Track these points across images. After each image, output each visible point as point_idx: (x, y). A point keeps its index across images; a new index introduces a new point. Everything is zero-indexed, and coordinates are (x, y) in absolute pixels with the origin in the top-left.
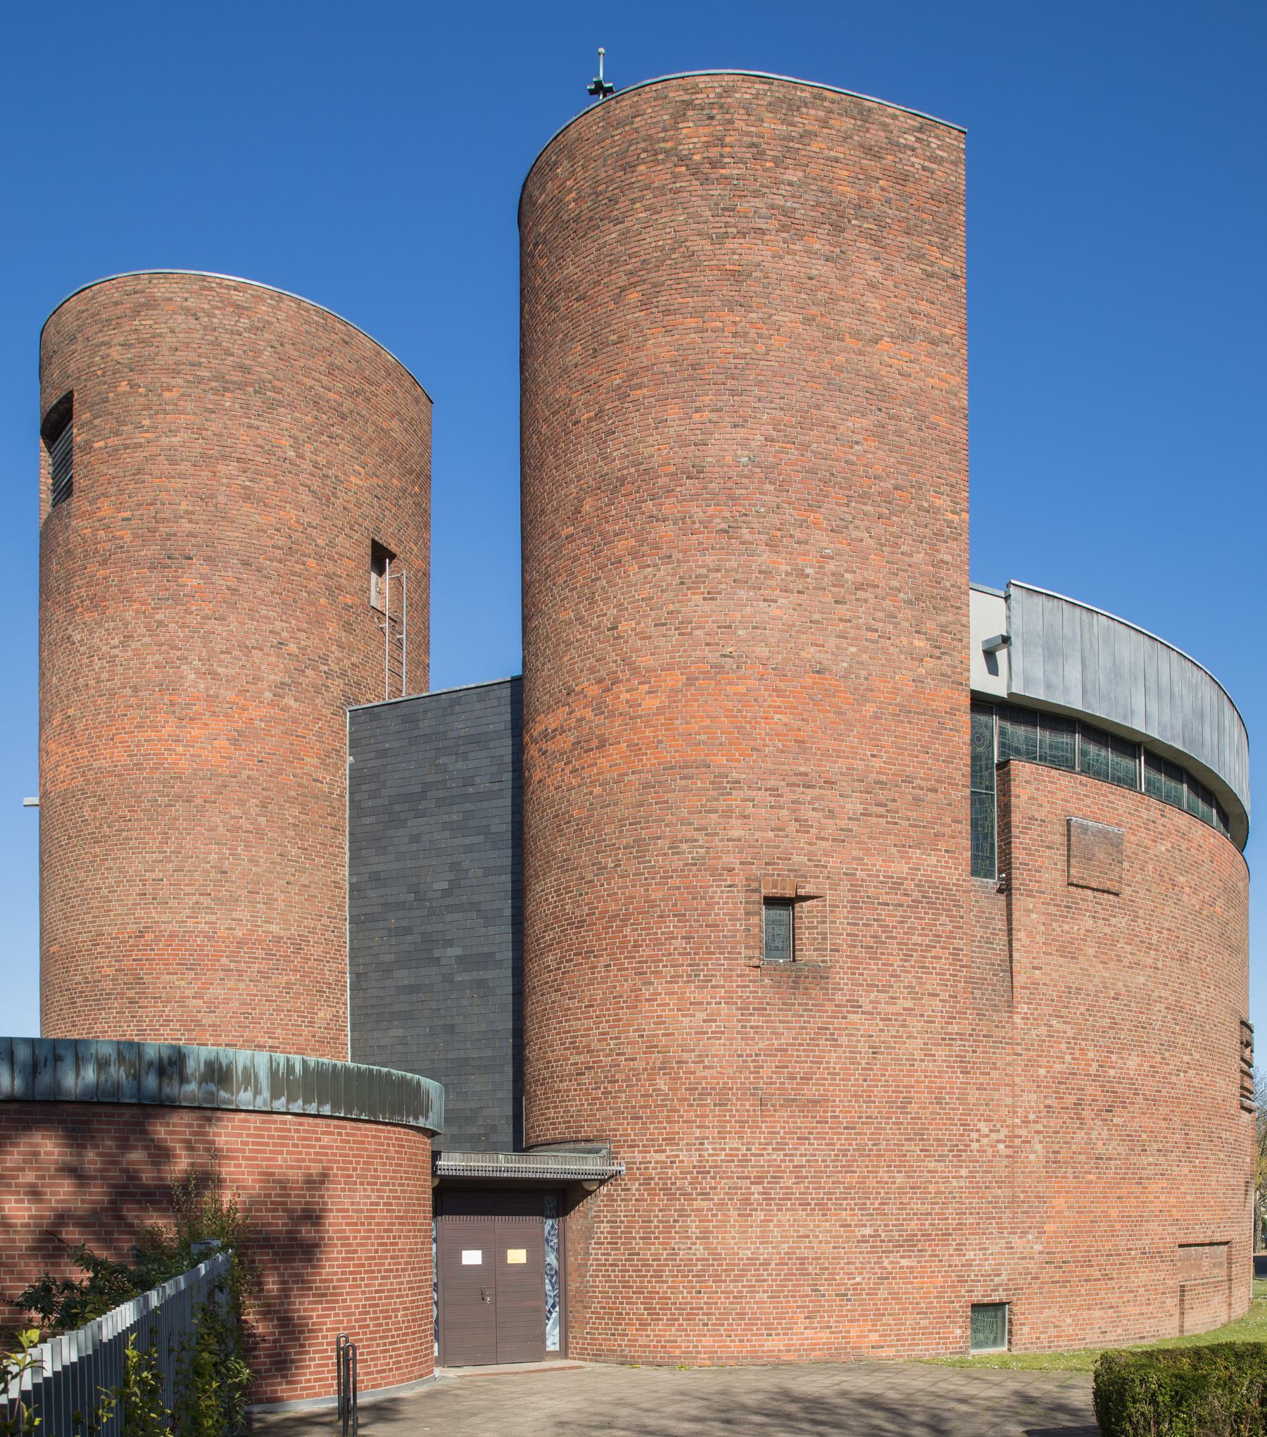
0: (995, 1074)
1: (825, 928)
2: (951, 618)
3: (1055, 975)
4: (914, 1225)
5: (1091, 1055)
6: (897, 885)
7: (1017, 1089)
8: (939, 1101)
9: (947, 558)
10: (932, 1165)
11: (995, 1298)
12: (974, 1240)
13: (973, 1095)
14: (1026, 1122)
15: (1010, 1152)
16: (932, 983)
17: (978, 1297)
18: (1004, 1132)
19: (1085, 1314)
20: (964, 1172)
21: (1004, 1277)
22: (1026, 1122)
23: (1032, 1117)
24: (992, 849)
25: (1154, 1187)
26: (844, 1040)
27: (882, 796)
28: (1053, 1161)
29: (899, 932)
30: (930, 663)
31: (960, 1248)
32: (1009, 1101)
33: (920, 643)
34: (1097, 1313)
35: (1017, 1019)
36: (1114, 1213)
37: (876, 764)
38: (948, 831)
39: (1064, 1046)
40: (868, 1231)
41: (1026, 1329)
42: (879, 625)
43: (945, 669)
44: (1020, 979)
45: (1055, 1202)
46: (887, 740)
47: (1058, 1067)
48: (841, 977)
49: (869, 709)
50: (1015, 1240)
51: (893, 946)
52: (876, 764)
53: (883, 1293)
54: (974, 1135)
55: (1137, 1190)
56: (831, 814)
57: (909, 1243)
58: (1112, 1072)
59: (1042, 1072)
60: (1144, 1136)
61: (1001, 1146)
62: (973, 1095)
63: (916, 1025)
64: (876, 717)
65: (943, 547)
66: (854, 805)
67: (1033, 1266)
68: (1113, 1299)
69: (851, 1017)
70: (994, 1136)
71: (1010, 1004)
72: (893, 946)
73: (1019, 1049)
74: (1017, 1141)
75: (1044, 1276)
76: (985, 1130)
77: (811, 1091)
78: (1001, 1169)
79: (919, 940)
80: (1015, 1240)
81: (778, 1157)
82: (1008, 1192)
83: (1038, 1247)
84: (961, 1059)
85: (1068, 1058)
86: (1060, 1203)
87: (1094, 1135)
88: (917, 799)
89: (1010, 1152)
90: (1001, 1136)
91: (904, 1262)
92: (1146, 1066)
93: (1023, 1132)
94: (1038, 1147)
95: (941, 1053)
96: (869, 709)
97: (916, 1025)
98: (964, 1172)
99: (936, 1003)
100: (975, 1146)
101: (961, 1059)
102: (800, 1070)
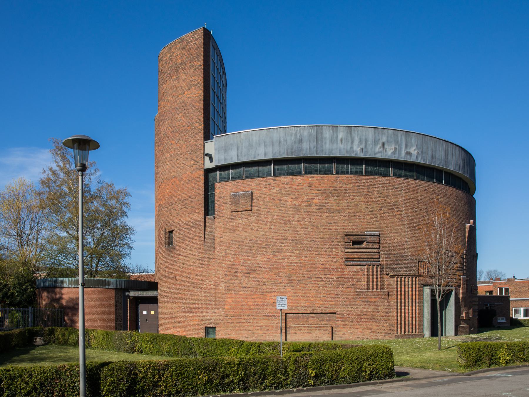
0: (210, 267)
1: (176, 236)
2: (199, 153)
3: (227, 238)
4: (192, 306)
5: (240, 258)
6: (187, 224)
7: (216, 270)
8: (197, 275)
9: (198, 138)
10: (195, 291)
11: (211, 325)
12: (205, 310)
13: (205, 273)
14: (219, 279)
15: (214, 287)
16: (195, 246)
17: (206, 325)
18: (213, 282)
19: (240, 332)
20: (202, 293)
21: (213, 320)
22: (219, 279)
23: (221, 277)
24: (208, 209)
25: (269, 295)
26: (178, 263)
27: (185, 202)
28: (227, 289)
29: (188, 235)
30: (194, 166)
31: (202, 312)
32: (214, 274)
33: (192, 162)
34: (244, 332)
35: (216, 252)
36: (251, 303)
37: (183, 195)
38: (198, 207)
39: (230, 257)
40: (183, 307)
41: (220, 334)
42: (184, 162)
43: (198, 167)
44: (217, 241)
45: (228, 300)
46: (185, 189)
47: (229, 263)
48: (177, 248)
49: (182, 182)
50: (216, 311)
51: (187, 238)
52: (183, 195)
53: (186, 323)
54: (205, 283)
55: (262, 296)
56: (176, 210)
57: (190, 311)
58: (249, 262)
59: (224, 265)
60: (264, 280)
61: (212, 286)
62: (205, 273)
63: (191, 257)
64: (183, 184)
65: (197, 136)
66: (179, 207)
67: (221, 318)
68: (251, 328)
69: (180, 257)
70: (210, 283)
71: (214, 248)
72: (187, 238)
73: (216, 260)
74: (216, 284)
75: (225, 320)
76: (208, 282)
77: (173, 275)
78: (212, 292)
79: (191, 236)
80: (216, 311)
81: (168, 290)
82: (214, 298)
83: (223, 312)
84: (202, 264)
85: (232, 260)
86: (230, 300)
87: (242, 281)
88: (192, 201)
89: (214, 287)
90: (212, 283)
91: (190, 315)
92: (265, 259)
93: (218, 282)
94: (222, 285)
95: (197, 263)
96: (182, 182)
97: (191, 257)
98: (202, 293)
99: (196, 251)
100: (205, 286)
101: (202, 264)
102: (171, 270)
